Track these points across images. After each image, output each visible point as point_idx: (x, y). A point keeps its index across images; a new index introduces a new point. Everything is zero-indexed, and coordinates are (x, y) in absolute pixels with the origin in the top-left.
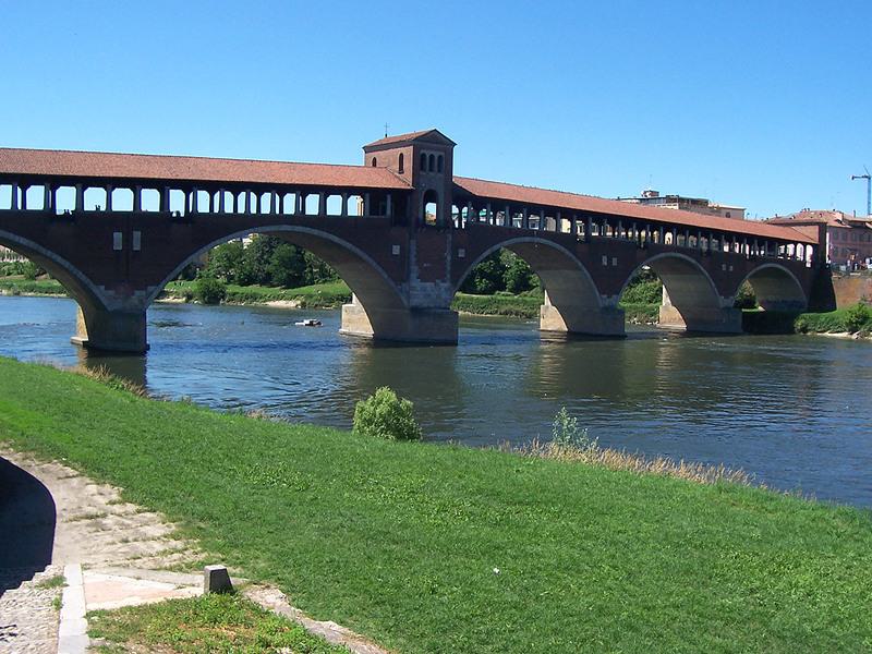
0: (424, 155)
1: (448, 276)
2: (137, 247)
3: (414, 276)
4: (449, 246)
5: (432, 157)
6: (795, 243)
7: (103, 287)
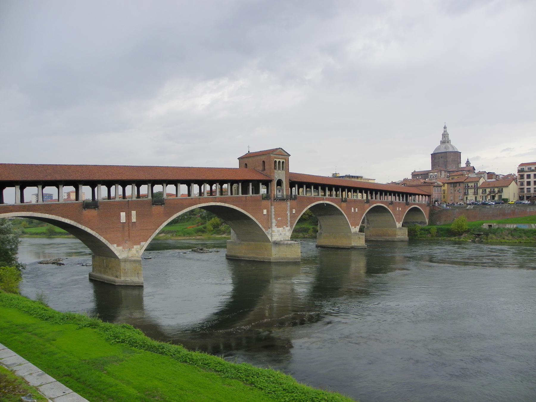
0: (275, 161)
1: (289, 223)
2: (134, 220)
3: (274, 224)
4: (289, 208)
5: (279, 162)
6: (419, 195)
7: (115, 245)
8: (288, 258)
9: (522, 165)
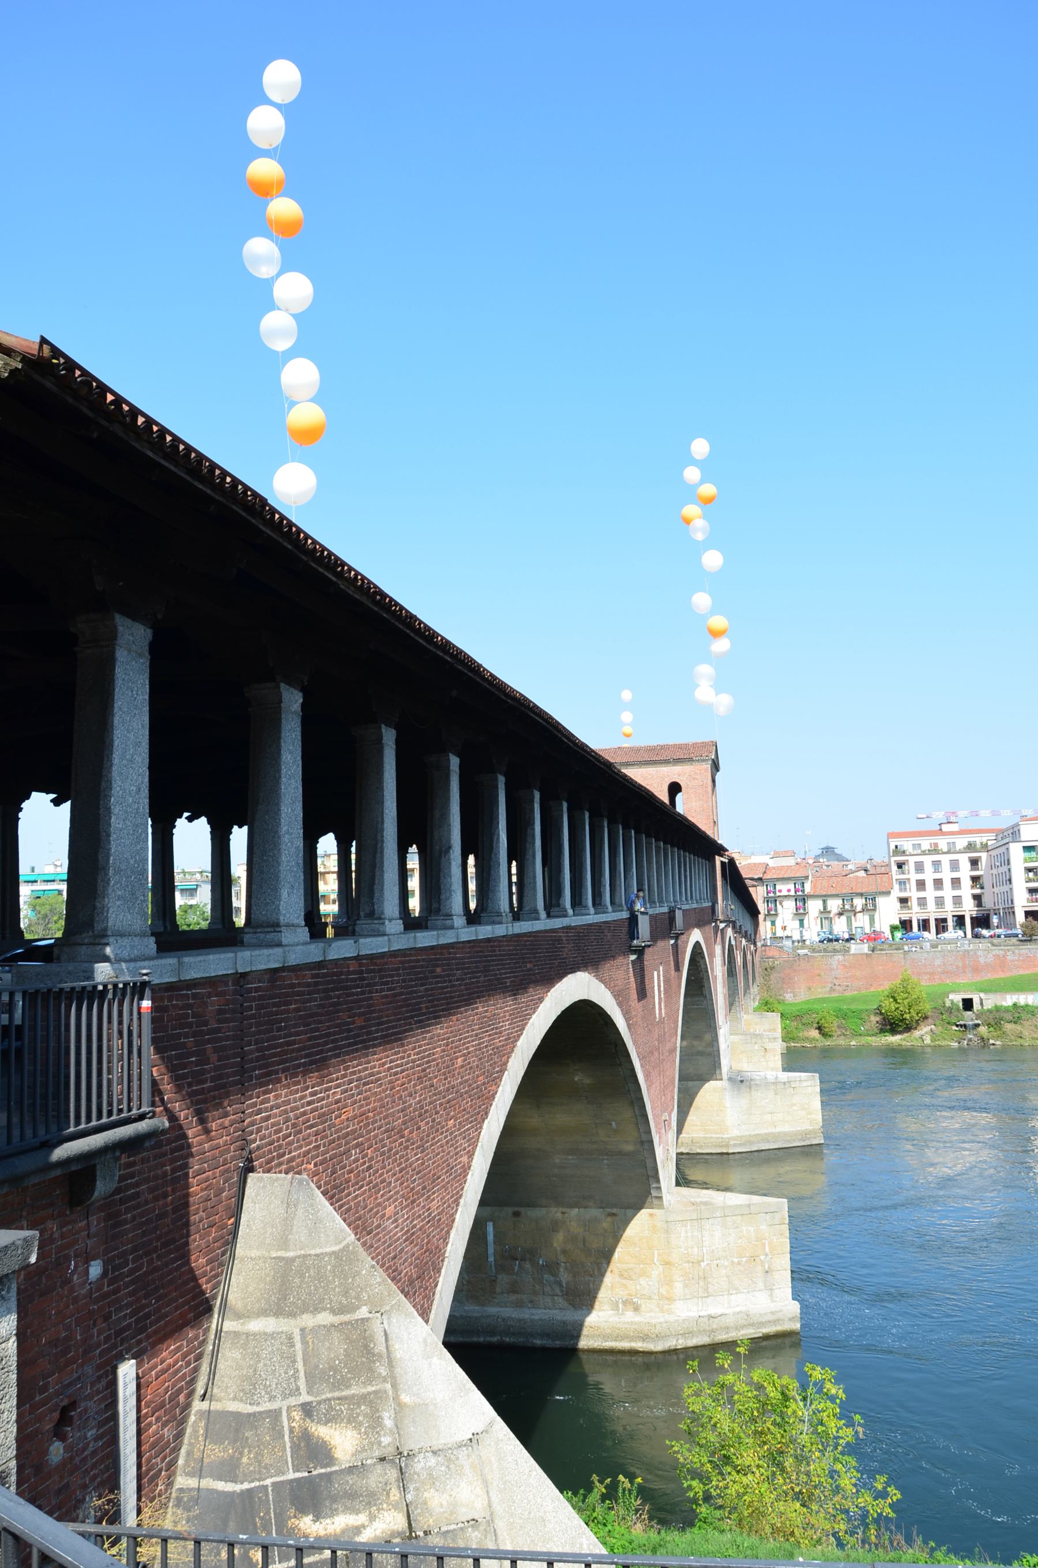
8: (785, 1134)
9: (892, 835)
